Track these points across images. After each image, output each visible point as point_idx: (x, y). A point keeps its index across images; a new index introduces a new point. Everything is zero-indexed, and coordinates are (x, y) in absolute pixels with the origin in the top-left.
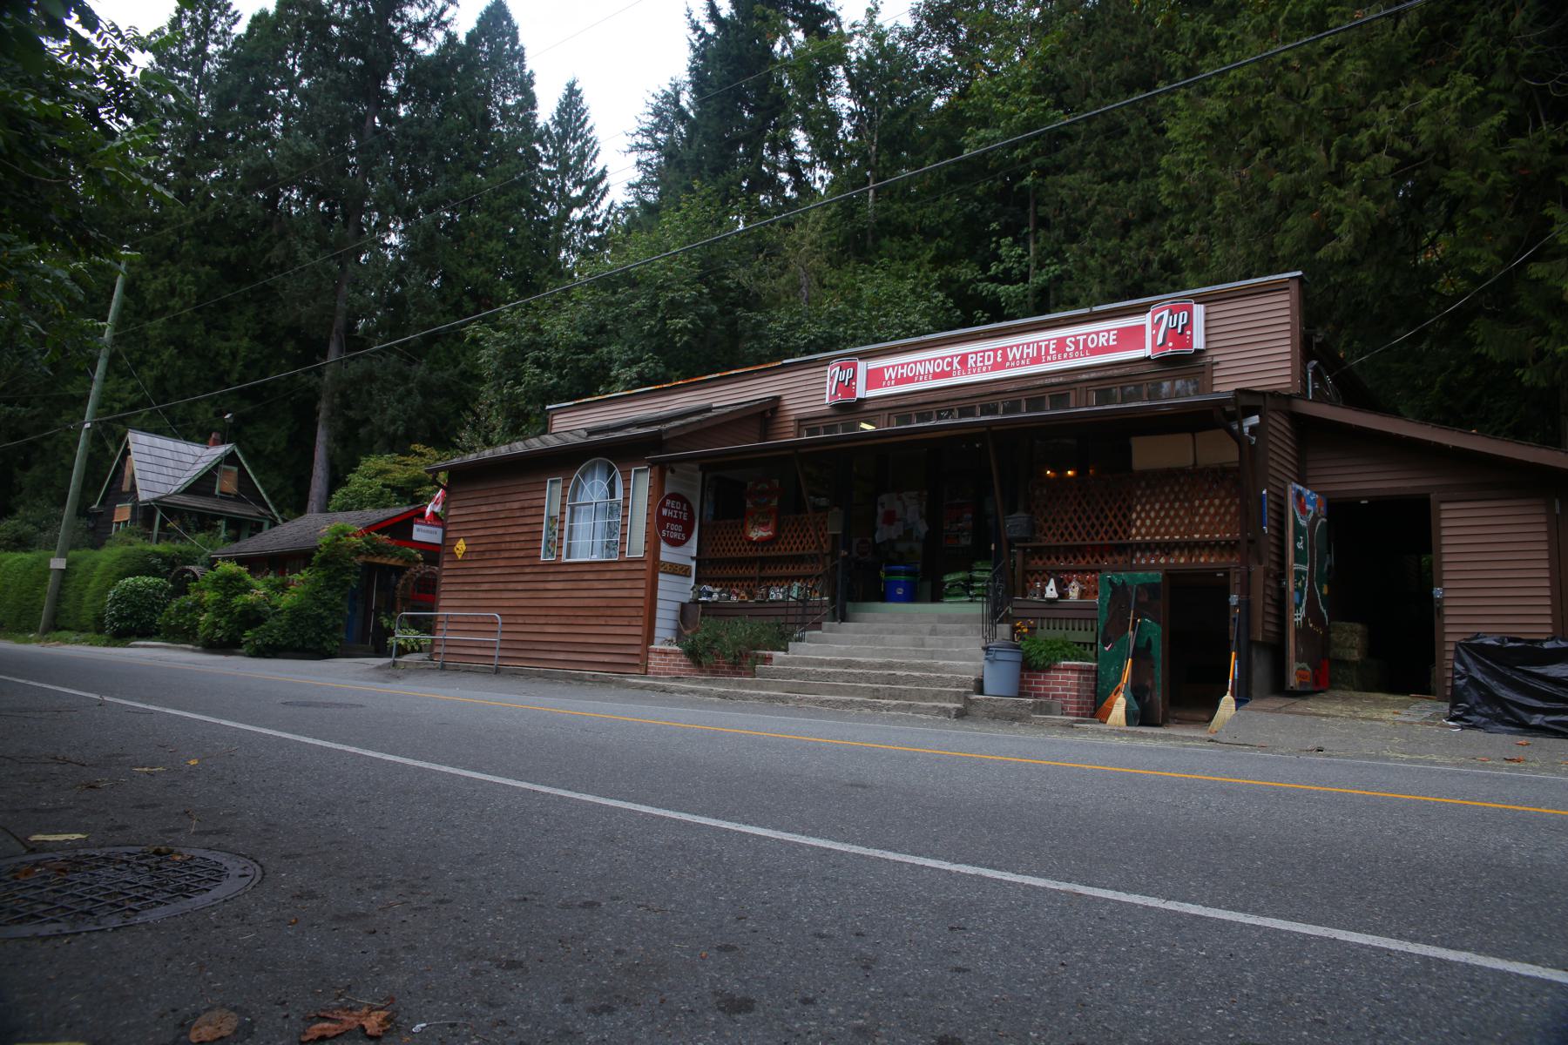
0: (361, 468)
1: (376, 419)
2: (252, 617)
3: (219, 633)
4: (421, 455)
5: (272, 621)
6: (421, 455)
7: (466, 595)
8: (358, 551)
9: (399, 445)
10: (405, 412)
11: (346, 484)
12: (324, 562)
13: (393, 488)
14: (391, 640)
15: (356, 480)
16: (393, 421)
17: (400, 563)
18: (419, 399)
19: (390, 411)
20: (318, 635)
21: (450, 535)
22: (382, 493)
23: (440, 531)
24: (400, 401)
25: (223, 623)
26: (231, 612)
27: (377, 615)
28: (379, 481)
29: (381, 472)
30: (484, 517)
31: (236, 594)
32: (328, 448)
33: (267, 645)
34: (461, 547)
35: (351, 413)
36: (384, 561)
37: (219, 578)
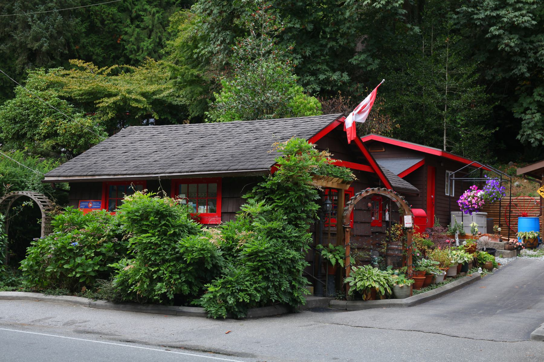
1: (18, 36)
3: (160, 288)
4: (82, 69)
6: (82, 69)
9: (59, 58)
10: (47, 29)
11: (13, 96)
13: (70, 100)
16: (36, 39)
17: (335, 186)
18: (60, 18)
19: (35, 28)
22: (59, 104)
24: (41, 18)
28: (53, 93)
29: (51, 85)
37: (145, 216)
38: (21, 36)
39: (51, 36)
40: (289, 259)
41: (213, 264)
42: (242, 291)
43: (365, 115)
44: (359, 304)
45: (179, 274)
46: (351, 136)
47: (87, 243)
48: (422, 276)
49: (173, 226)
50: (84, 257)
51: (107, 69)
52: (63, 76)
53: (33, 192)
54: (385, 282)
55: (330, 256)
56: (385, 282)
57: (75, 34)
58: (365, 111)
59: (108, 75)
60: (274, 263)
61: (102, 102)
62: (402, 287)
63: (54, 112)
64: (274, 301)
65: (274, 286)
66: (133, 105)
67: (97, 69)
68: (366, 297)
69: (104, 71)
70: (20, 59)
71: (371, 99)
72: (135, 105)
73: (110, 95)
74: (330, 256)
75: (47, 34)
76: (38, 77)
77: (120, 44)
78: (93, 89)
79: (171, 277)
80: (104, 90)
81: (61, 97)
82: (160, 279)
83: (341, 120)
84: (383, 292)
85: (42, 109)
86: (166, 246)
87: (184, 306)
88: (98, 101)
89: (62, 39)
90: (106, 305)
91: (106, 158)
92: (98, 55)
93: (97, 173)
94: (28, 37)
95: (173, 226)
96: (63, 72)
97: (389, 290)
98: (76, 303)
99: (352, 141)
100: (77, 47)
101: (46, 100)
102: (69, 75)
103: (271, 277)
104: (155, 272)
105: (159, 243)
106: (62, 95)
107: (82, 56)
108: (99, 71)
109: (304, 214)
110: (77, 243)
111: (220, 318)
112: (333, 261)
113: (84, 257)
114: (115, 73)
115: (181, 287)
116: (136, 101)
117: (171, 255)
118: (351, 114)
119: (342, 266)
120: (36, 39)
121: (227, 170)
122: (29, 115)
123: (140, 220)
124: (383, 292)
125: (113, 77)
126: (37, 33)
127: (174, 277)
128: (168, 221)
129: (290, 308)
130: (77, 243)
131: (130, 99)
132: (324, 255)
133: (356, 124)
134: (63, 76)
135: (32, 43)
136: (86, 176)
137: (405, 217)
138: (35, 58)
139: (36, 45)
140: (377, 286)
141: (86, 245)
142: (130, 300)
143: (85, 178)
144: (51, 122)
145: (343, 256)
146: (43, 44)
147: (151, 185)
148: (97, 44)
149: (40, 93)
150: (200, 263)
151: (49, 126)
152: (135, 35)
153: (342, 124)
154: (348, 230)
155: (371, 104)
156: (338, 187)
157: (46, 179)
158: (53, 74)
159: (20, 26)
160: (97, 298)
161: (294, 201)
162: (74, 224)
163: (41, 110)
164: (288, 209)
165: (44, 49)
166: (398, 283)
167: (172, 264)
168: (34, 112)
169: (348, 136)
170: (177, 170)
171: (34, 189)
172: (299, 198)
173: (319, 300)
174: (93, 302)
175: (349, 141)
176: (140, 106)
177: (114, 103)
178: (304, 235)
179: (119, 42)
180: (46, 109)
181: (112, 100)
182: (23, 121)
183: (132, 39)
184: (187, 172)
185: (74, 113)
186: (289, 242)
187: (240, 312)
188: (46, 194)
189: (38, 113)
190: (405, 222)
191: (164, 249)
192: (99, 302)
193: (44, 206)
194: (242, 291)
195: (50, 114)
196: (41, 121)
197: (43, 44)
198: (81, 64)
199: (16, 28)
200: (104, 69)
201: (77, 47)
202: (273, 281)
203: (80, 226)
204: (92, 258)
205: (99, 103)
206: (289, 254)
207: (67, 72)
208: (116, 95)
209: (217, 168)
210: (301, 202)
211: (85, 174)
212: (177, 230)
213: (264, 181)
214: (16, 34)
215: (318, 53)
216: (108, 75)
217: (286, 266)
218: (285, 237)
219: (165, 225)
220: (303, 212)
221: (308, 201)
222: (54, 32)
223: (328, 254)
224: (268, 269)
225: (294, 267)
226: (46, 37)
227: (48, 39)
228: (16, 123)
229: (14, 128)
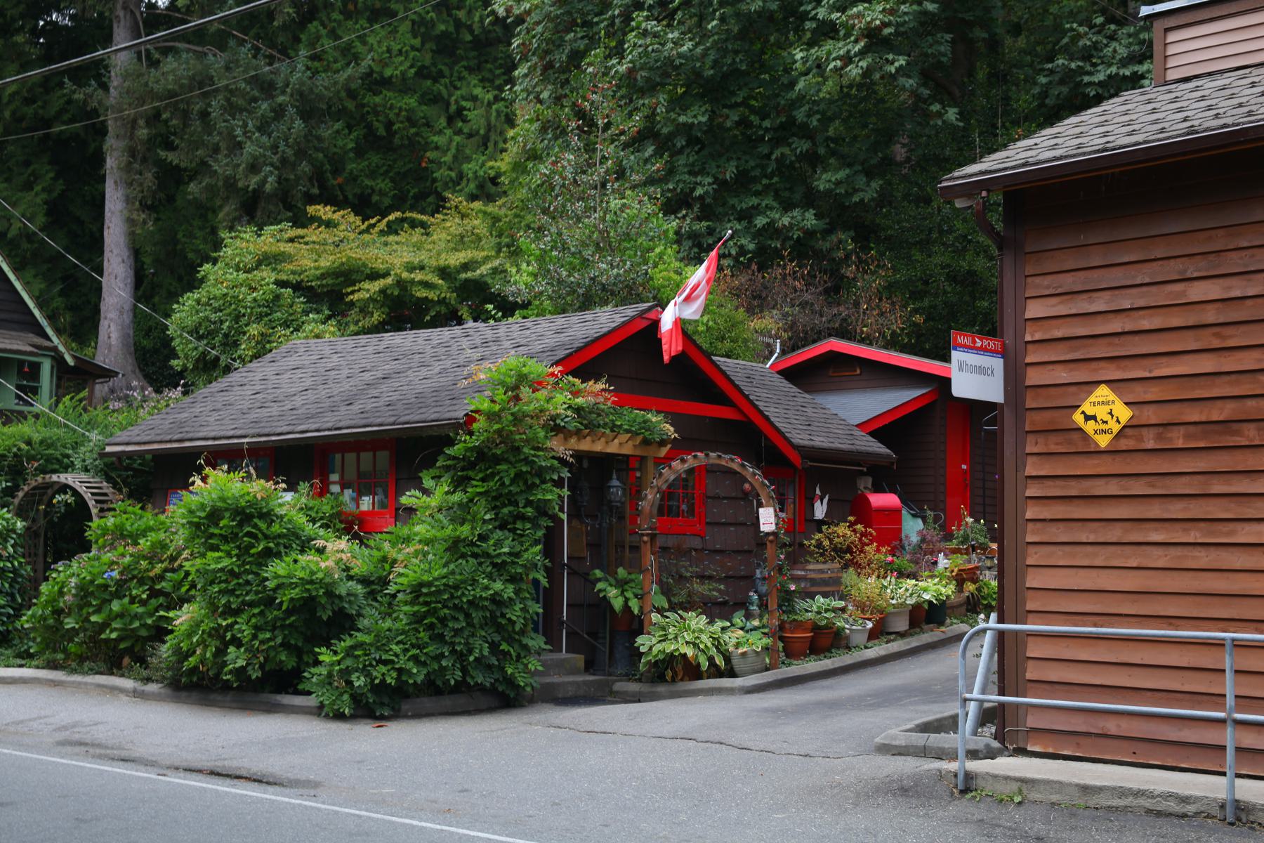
0: (227, 252)
1: (221, 166)
2: (320, 618)
3: (236, 658)
4: (329, 224)
5: (371, 619)
6: (329, 224)
7: (1160, 558)
8: (555, 427)
9: (285, 206)
10: (275, 148)
12: (482, 459)
13: (297, 287)
14: (643, 642)
15: (218, 278)
16: (254, 168)
17: (627, 450)
18: (298, 123)
19: (249, 148)
20: (494, 646)
21: (1034, 377)
22: (277, 297)
23: (997, 364)
24: (263, 128)
25: (244, 628)
26: (269, 602)
27: (583, 578)
28: (267, 275)
29: (268, 260)
30: (1210, 316)
31: (269, 554)
32: (131, 222)
33: (380, 688)
34: (1104, 411)
35: (171, 157)
36: (598, 447)
37: (214, 515)
38: (227, 165)
39: (284, 161)
40: (486, 599)
41: (333, 611)
42: (385, 662)
43: (698, 304)
44: (661, 689)
45: (273, 630)
46: (671, 347)
47: (136, 572)
48: (805, 631)
49: (266, 537)
50: (126, 600)
51: (379, 221)
52: (291, 240)
53: (84, 477)
54: (709, 645)
55: (613, 592)
56: (709, 645)
57: (335, 154)
58: (698, 297)
59: (382, 233)
60: (455, 607)
61: (359, 290)
62: (744, 654)
63: (267, 315)
64: (453, 682)
65: (453, 652)
66: (418, 294)
67: (359, 223)
68: (675, 675)
69: (374, 226)
70: (226, 209)
71: (707, 271)
72: (421, 293)
73: (374, 276)
74: (613, 592)
75: (275, 159)
76: (244, 243)
77: (426, 168)
78: (343, 264)
79: (255, 637)
80: (365, 265)
81: (281, 284)
82: (237, 642)
83: (651, 315)
84: (705, 665)
85: (246, 307)
86: (250, 577)
87: (287, 693)
88: (349, 290)
89: (305, 167)
90: (160, 694)
91: (219, 406)
92: (381, 193)
93: (190, 436)
94: (239, 165)
95: (266, 537)
96: (292, 233)
97: (719, 661)
98: (113, 689)
99: (673, 359)
100: (340, 180)
101: (254, 290)
102: (303, 237)
103: (448, 635)
104: (230, 626)
105: (236, 570)
106: (285, 278)
107: (350, 197)
108: (363, 227)
109: (529, 509)
110: (115, 574)
111: (339, 716)
112: (618, 604)
113: (126, 600)
114: (392, 229)
115: (277, 654)
116: (426, 285)
117: (257, 593)
118: (672, 303)
119: (636, 612)
120: (254, 168)
121: (393, 424)
122: (222, 322)
123: (207, 526)
124: (705, 665)
125: (392, 238)
126: (255, 158)
127: (261, 636)
128: (255, 526)
129: (505, 698)
130: (115, 574)
131: (412, 282)
132: (600, 591)
133: (679, 323)
134: (291, 240)
135: (246, 177)
136: (170, 441)
137: (761, 510)
138: (254, 210)
139: (254, 181)
140: (690, 652)
141: (134, 577)
142: (199, 685)
143: (169, 446)
144: (262, 334)
145: (640, 592)
146: (266, 177)
147: (229, 456)
148: (382, 171)
149: (242, 276)
150: (307, 605)
151: (258, 343)
152: (453, 151)
153: (656, 323)
154: (645, 538)
155: (708, 282)
156: (638, 453)
157: (108, 449)
158: (271, 238)
159: (223, 145)
160: (148, 680)
161: (507, 482)
162: (123, 537)
163: (243, 311)
164: (497, 500)
165: (268, 187)
166: (737, 646)
167: (256, 611)
168: (229, 314)
169: (665, 347)
170: (314, 427)
171: (86, 470)
172: (519, 475)
173: (585, 683)
174: (138, 685)
175: (666, 358)
176: (432, 295)
177: (383, 291)
178: (527, 550)
179: (424, 165)
180: (252, 308)
181: (375, 286)
182: (211, 334)
183: (448, 158)
184: (329, 430)
185: (306, 313)
186: (494, 565)
187: (382, 704)
188: (109, 479)
189: (238, 318)
190: (762, 521)
191: (248, 583)
192: (153, 687)
193: (97, 501)
194: (385, 662)
195: (260, 317)
196: (244, 333)
197: (266, 177)
198: (330, 215)
199: (216, 150)
200: (373, 221)
201: (340, 180)
202: (453, 644)
203: (134, 538)
204: (143, 603)
205: (353, 293)
206: (487, 588)
207: (300, 232)
208: (386, 275)
209: (379, 421)
210: (526, 482)
211: (168, 438)
212: (271, 545)
213: (451, 443)
214: (216, 161)
215: (757, 172)
216: (382, 233)
217: (480, 614)
218: (488, 555)
219: (249, 534)
220: (529, 503)
221: (538, 482)
222: (289, 152)
223: (609, 588)
224: (443, 621)
225: (503, 615)
226: (272, 165)
227: (276, 168)
228: (200, 338)
229: (196, 349)
